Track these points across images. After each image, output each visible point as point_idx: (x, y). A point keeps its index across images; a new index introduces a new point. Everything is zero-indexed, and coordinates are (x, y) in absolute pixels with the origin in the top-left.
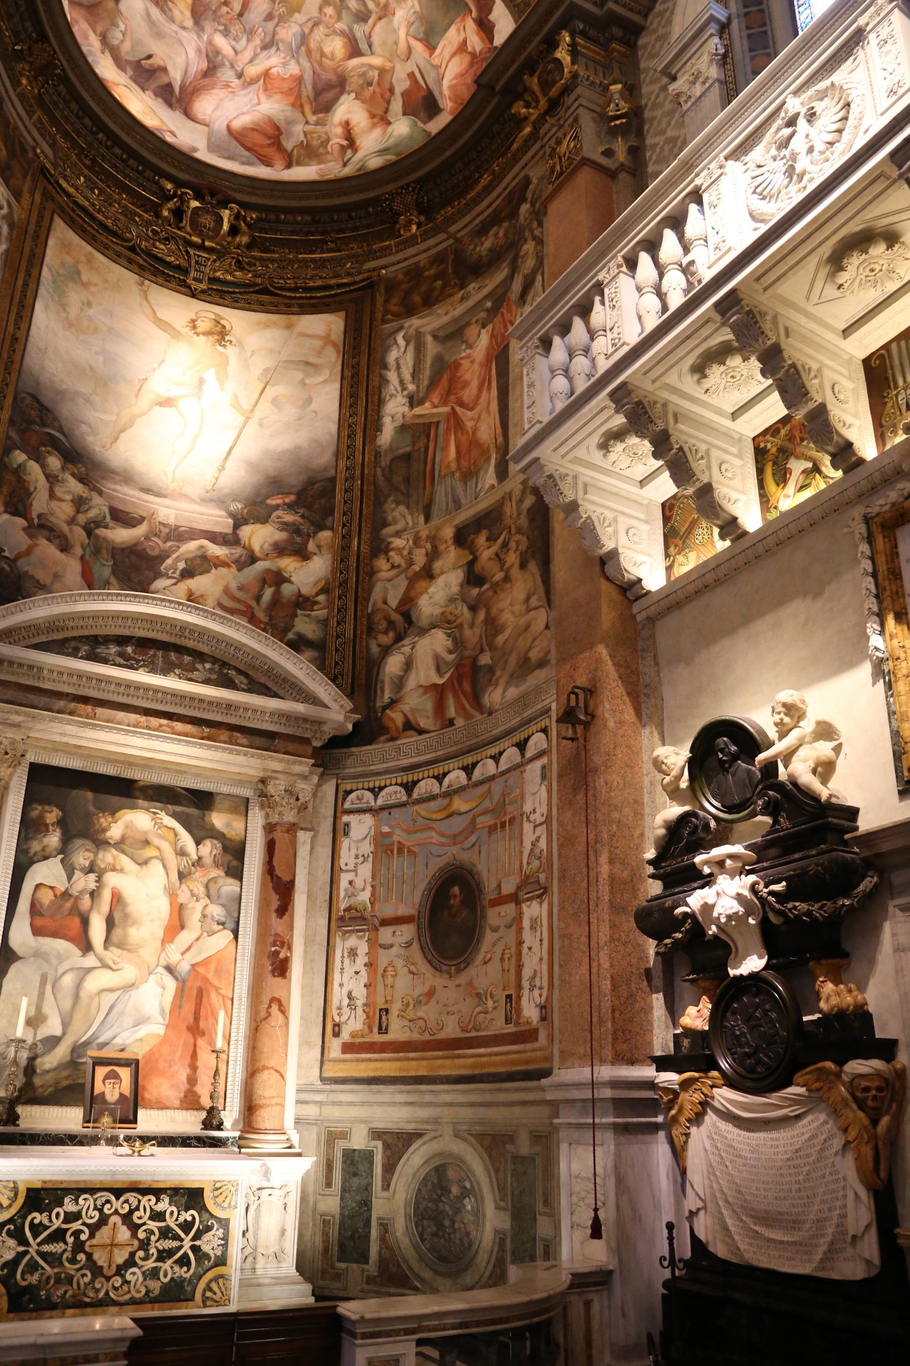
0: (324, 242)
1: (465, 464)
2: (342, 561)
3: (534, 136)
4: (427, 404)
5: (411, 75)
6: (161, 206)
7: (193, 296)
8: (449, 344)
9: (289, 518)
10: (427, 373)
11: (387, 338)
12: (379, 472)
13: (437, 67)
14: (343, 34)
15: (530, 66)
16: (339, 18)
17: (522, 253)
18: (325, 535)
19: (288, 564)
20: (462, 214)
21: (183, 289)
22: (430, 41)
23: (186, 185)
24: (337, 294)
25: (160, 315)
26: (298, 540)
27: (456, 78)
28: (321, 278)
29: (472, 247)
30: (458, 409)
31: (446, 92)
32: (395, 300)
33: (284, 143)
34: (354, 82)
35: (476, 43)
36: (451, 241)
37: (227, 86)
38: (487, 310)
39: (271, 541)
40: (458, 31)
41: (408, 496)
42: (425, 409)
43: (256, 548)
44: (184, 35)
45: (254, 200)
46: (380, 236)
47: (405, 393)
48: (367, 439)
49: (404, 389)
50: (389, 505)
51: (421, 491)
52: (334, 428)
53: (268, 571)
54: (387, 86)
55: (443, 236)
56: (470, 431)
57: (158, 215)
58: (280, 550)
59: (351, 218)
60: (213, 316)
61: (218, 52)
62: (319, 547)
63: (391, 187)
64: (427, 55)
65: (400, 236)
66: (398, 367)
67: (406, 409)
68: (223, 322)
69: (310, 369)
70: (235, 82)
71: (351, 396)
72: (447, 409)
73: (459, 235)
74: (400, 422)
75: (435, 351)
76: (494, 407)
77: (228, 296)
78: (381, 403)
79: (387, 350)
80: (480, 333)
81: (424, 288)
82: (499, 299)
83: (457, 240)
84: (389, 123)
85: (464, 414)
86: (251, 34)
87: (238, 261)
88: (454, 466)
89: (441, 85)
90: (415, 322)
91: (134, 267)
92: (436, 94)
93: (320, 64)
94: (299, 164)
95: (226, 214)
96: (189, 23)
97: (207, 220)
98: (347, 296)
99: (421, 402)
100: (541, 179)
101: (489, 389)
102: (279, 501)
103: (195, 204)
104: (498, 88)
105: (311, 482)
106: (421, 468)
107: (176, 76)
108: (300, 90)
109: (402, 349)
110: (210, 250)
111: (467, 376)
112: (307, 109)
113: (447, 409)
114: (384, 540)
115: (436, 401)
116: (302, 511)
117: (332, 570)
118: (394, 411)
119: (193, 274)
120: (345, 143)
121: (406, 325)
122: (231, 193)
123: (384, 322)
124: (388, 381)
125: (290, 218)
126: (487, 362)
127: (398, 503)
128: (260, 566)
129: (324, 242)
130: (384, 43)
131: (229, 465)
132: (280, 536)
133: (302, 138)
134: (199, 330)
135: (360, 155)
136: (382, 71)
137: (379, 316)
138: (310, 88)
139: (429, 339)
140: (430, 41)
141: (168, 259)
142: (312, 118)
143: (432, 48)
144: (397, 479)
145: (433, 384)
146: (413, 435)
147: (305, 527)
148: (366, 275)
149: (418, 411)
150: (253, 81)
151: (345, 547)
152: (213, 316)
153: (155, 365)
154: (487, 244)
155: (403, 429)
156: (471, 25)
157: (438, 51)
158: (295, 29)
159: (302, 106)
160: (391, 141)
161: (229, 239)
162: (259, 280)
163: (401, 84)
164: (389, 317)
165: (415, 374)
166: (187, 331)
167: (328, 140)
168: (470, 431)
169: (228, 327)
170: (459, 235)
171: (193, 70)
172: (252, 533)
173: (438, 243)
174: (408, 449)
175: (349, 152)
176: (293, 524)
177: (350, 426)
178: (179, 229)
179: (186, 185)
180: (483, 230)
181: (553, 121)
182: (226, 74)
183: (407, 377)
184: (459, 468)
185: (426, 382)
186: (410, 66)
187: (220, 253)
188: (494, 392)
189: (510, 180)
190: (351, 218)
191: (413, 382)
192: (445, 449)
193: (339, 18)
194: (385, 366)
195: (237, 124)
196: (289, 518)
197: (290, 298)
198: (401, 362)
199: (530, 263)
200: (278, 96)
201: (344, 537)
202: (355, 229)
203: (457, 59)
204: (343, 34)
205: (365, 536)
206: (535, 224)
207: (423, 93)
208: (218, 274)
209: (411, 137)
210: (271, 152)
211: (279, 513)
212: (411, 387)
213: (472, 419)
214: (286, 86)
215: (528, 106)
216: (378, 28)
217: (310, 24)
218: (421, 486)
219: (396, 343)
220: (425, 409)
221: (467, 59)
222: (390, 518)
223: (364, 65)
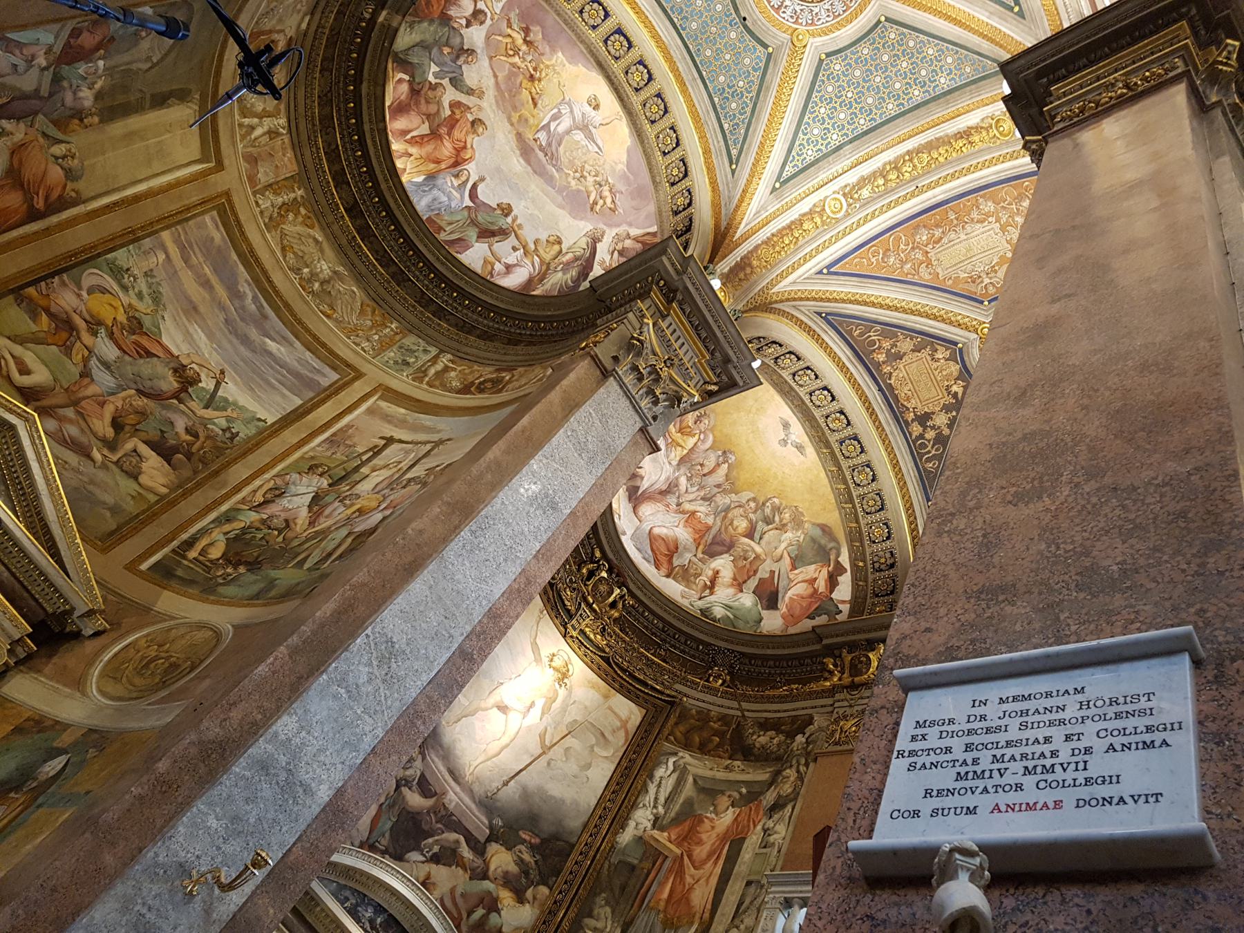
0: (660, 646)
1: (671, 911)
2: (544, 923)
3: (832, 691)
4: (666, 834)
5: (773, 572)
6: (585, 562)
7: (564, 637)
8: (702, 796)
9: (527, 857)
10: (676, 808)
11: (663, 755)
12: (606, 866)
13: (791, 581)
14: (751, 521)
15: (852, 646)
16: (755, 512)
17: (784, 773)
18: (544, 890)
19: (506, 897)
20: (756, 700)
21: (562, 628)
22: (796, 563)
23: (608, 561)
24: (647, 694)
25: (537, 640)
26: (524, 880)
27: (797, 595)
28: (645, 674)
29: (750, 731)
30: (686, 858)
31: (787, 599)
32: (682, 728)
33: (674, 559)
34: (738, 550)
35: (821, 585)
36: (739, 713)
38: (740, 793)
39: (505, 868)
40: (816, 570)
41: (618, 903)
42: (662, 837)
43: (492, 867)
45: (638, 593)
46: (694, 670)
47: (655, 811)
48: (612, 829)
49: (655, 807)
50: (600, 900)
51: (629, 907)
52: (594, 802)
53: (490, 893)
54: (755, 568)
55: (735, 704)
56: (687, 887)
57: (579, 570)
58: (507, 881)
59: (685, 643)
60: (566, 658)
62: (535, 898)
63: (723, 644)
64: (789, 568)
65: (708, 681)
66: (659, 786)
67: (649, 825)
68: (570, 666)
69: (602, 740)
71: (618, 784)
72: (678, 851)
73: (746, 713)
74: (639, 833)
75: (690, 793)
76: (714, 881)
77: (583, 649)
78: (634, 806)
79: (657, 764)
80: (728, 808)
81: (705, 734)
82: (752, 795)
83: (743, 716)
84: (742, 591)
85: (689, 868)
86: (702, 487)
87: (604, 628)
88: (662, 905)
89: (786, 593)
90: (686, 757)
91: (545, 598)
92: (780, 596)
93: (726, 528)
94: (674, 579)
95: (617, 591)
97: (603, 588)
98: (652, 699)
99: (662, 829)
100: (820, 729)
101: (716, 863)
102: (527, 838)
103: (604, 574)
104: (825, 642)
105: (556, 837)
106: (638, 887)
108: (704, 535)
109: (669, 772)
110: (594, 611)
111: (704, 837)
112: (701, 547)
113: (678, 851)
114: (582, 928)
115: (673, 837)
116: (538, 857)
117: (533, 926)
118: (641, 820)
119: (574, 622)
120: (708, 583)
121: (681, 754)
122: (629, 580)
123: (667, 739)
124: (647, 791)
125: (651, 617)
126: (723, 838)
127: (607, 903)
128: (487, 885)
129: (660, 646)
130: (769, 543)
131: (512, 782)
132: (513, 868)
133: (686, 563)
134: (553, 664)
135: (712, 598)
136: (757, 557)
137: (666, 732)
138: (711, 537)
139: (690, 779)
140: (796, 563)
141: (566, 602)
142: (700, 555)
143: (794, 568)
144: (617, 883)
145: (676, 821)
146: (645, 852)
147: (534, 874)
148: (673, 693)
149: (656, 833)
150: (683, 512)
151: (552, 913)
152: (566, 658)
153: (513, 676)
154: (763, 740)
155: (639, 840)
156: (824, 574)
157: (796, 572)
158: (727, 501)
159: (699, 544)
160: (736, 603)
161: (608, 609)
162: (607, 650)
163: (763, 573)
164: (672, 738)
165: (668, 800)
166: (546, 660)
167: (700, 575)
168: (687, 887)
169: (570, 673)
170: (746, 713)
171: (656, 486)
172: (497, 852)
173: (729, 707)
174: (636, 862)
175: (708, 591)
176: (527, 864)
177: (605, 809)
178: (585, 585)
179: (608, 561)
180: (765, 725)
181: (849, 697)
182: (672, 500)
183: (662, 800)
184: (665, 911)
185: (673, 814)
186: (775, 567)
187: (597, 616)
188: (718, 870)
189: (799, 708)
190: (685, 643)
191: (664, 806)
192: (662, 884)
193: (755, 512)
194: (651, 777)
195: (656, 531)
196: (527, 857)
197: (619, 675)
198: (663, 782)
199: (787, 789)
200: (691, 530)
201: (555, 902)
202: (683, 651)
203: (805, 585)
204: (751, 521)
205: (571, 914)
206: (803, 761)
207: (773, 589)
208: (587, 629)
209: (750, 610)
210: (663, 560)
211: (522, 848)
212: (661, 810)
213: (692, 876)
214: (699, 526)
215: (835, 665)
216: (771, 532)
217: (737, 504)
218: (630, 902)
219: (667, 763)
220: (662, 837)
221: (810, 591)
222: (595, 912)
223: (749, 546)
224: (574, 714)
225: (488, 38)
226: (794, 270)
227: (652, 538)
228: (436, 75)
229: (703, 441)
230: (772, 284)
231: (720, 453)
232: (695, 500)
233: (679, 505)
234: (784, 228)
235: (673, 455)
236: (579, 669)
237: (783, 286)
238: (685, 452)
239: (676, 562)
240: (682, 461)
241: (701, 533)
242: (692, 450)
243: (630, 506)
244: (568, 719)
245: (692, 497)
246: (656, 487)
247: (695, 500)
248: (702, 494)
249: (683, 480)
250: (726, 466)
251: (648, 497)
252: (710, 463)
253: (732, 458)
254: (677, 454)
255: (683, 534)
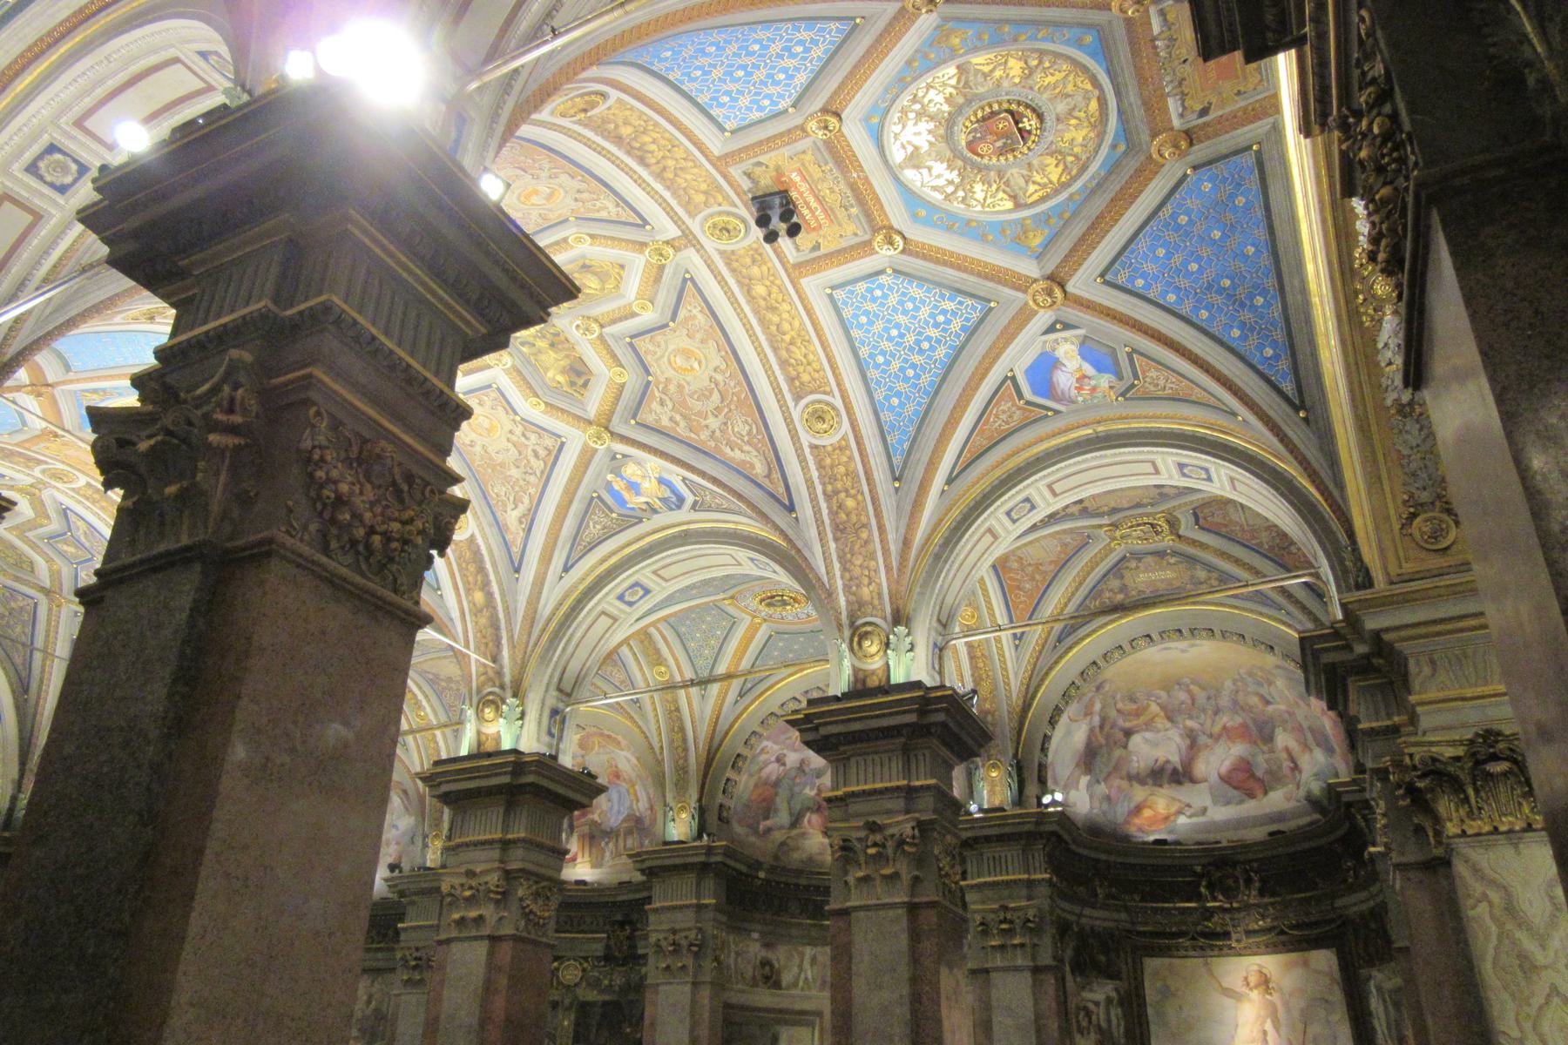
7: (1240, 955)
37: (1207, 746)
44: (1170, 733)
61: (1192, 730)
70: (1210, 741)
96: (1169, 725)
107: (1175, 759)
134: (1252, 984)
166: (1245, 990)
182: (1203, 739)
195: (1223, 770)
210: (1252, 784)
224: (1298, 1003)
225: (795, 751)
226: (1006, 670)
227: (1226, 779)
228: (812, 789)
229: (1158, 697)
230: (1009, 698)
231: (1177, 687)
232: (1213, 721)
233: (1211, 736)
234: (971, 663)
235: (1160, 726)
236: (1270, 963)
237: (1016, 685)
238: (1162, 714)
239: (1259, 773)
240: (1170, 719)
241: (1243, 733)
242: (1163, 708)
243: (1188, 786)
244: (1296, 1014)
245: (1209, 722)
246: (1184, 748)
247: (1213, 721)
248: (1210, 712)
249: (1189, 723)
250: (1192, 687)
251: (1188, 764)
252: (1183, 696)
253: (1186, 680)
254: (1161, 722)
255: (1238, 749)
